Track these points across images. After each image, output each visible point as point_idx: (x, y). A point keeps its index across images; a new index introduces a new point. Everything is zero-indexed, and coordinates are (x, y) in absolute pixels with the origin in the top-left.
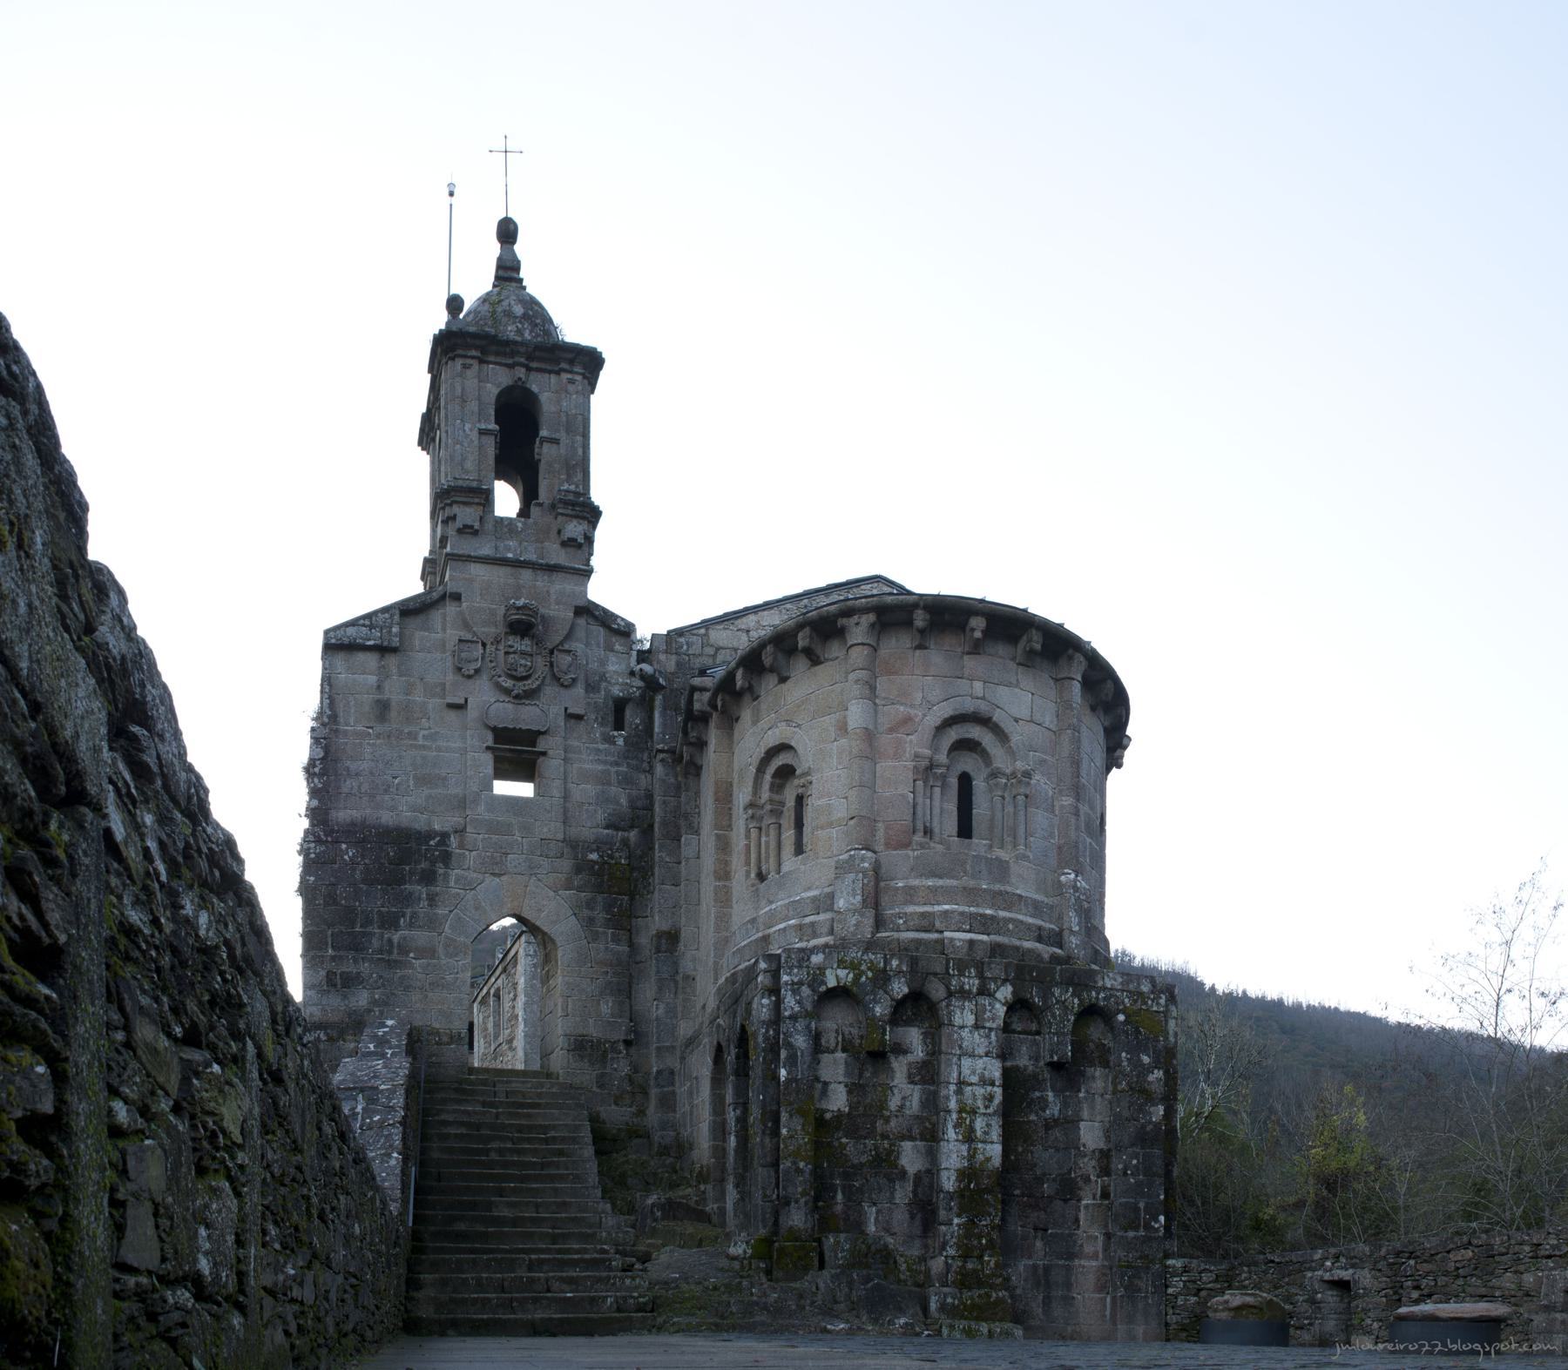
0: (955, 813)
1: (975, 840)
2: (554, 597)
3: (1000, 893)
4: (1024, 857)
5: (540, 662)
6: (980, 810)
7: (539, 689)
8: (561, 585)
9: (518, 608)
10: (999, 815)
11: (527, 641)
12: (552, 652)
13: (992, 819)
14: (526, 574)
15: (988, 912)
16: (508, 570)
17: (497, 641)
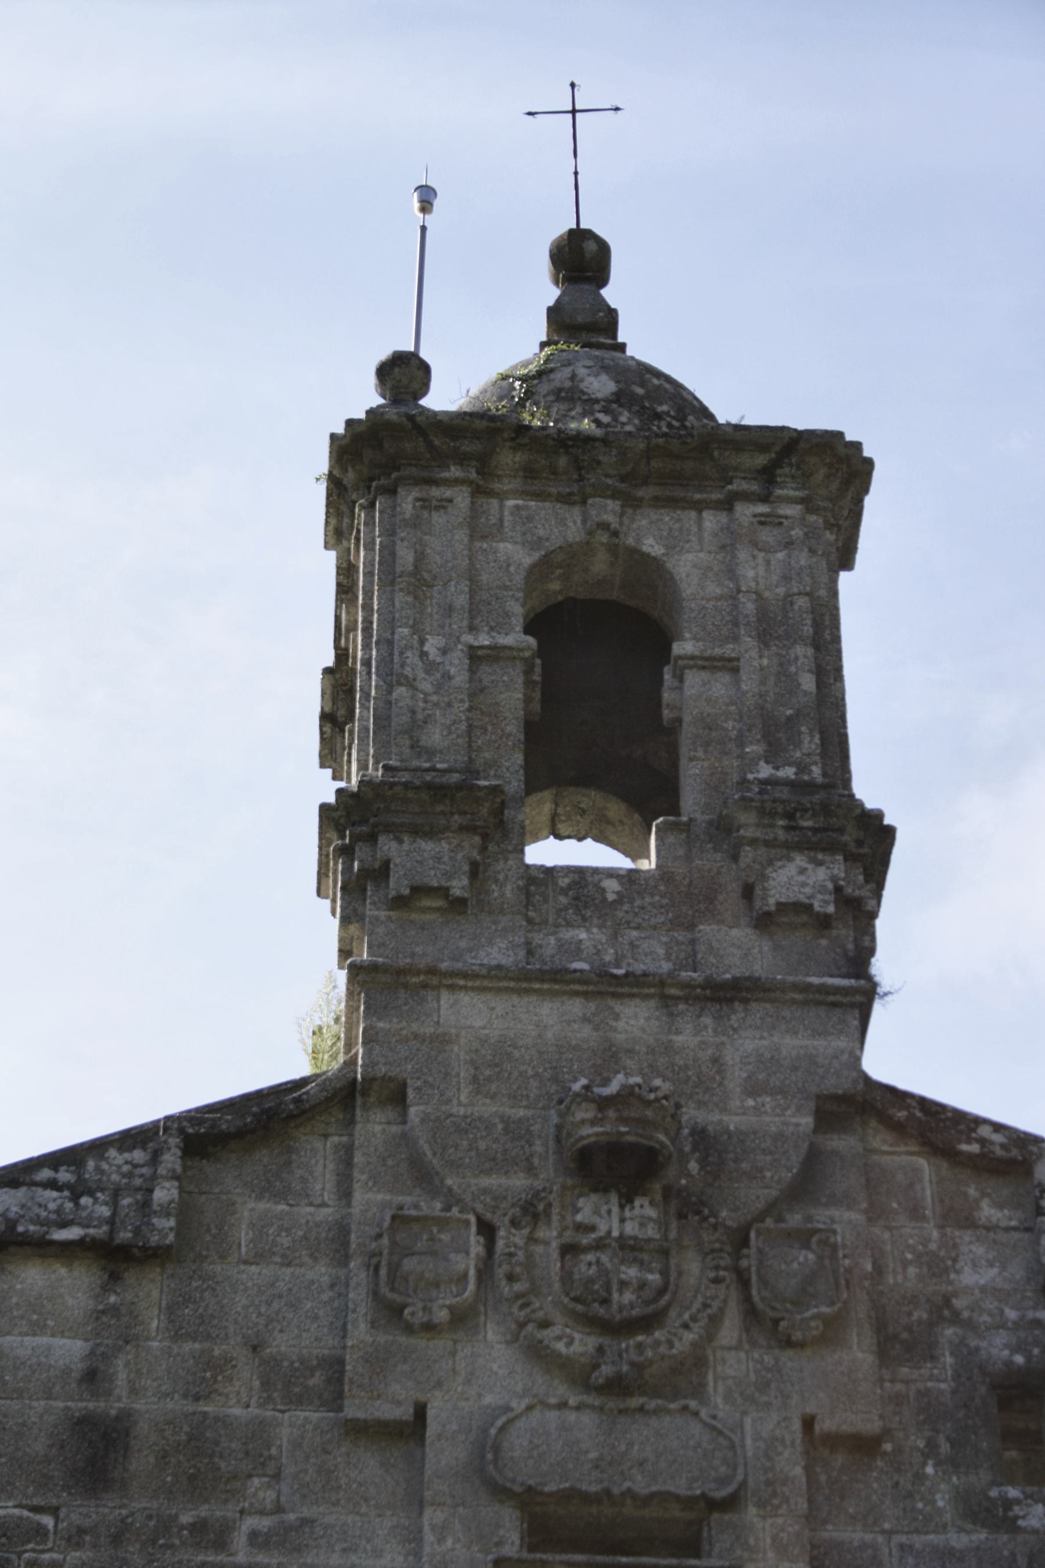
2: (736, 1077)
5: (692, 1266)
7: (697, 1362)
8: (749, 1041)
9: (604, 1103)
11: (644, 1208)
12: (741, 1240)
14: (635, 1020)
16: (576, 1007)
17: (532, 1211)
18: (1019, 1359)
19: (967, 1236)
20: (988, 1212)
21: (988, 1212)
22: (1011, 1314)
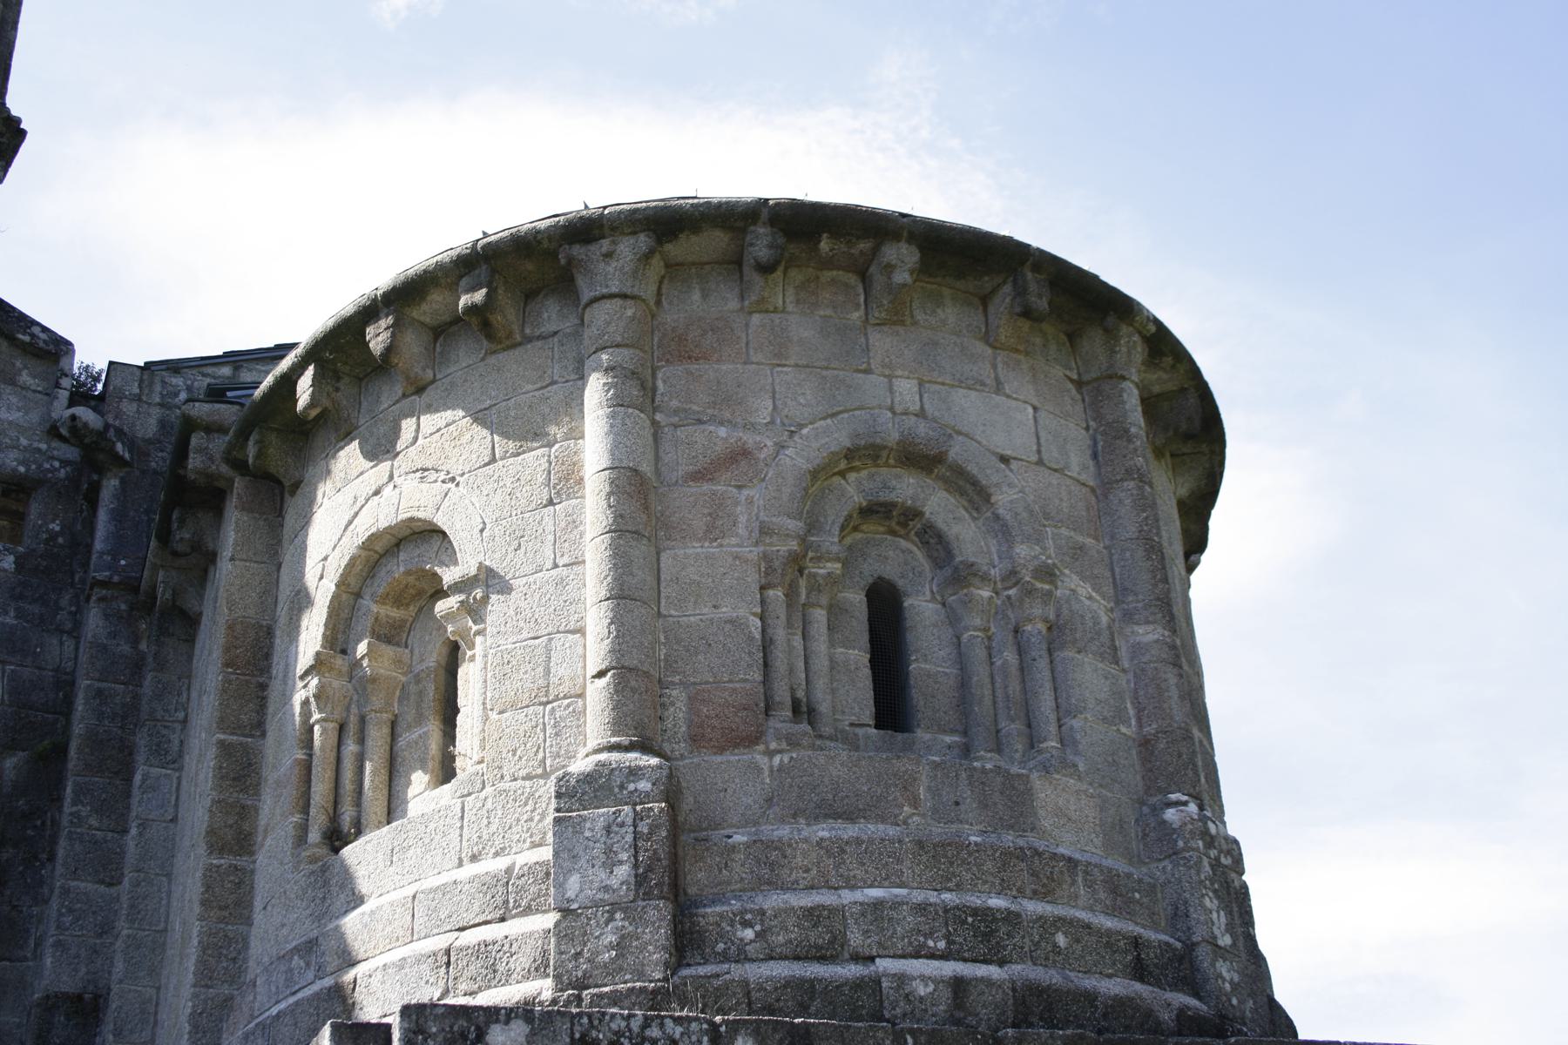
0: (866, 672)
1: (922, 735)
3: (1020, 854)
4: (1067, 766)
6: (929, 660)
10: (980, 673)
13: (964, 684)
15: (996, 902)
18: (22, 469)
19: (9, 389)
20: (25, 378)
21: (25, 378)
22: (24, 442)
